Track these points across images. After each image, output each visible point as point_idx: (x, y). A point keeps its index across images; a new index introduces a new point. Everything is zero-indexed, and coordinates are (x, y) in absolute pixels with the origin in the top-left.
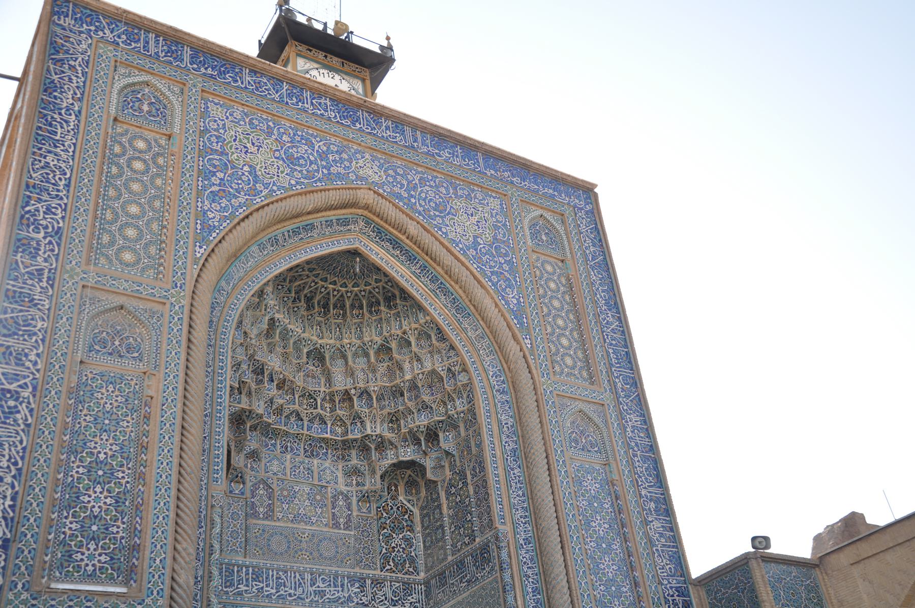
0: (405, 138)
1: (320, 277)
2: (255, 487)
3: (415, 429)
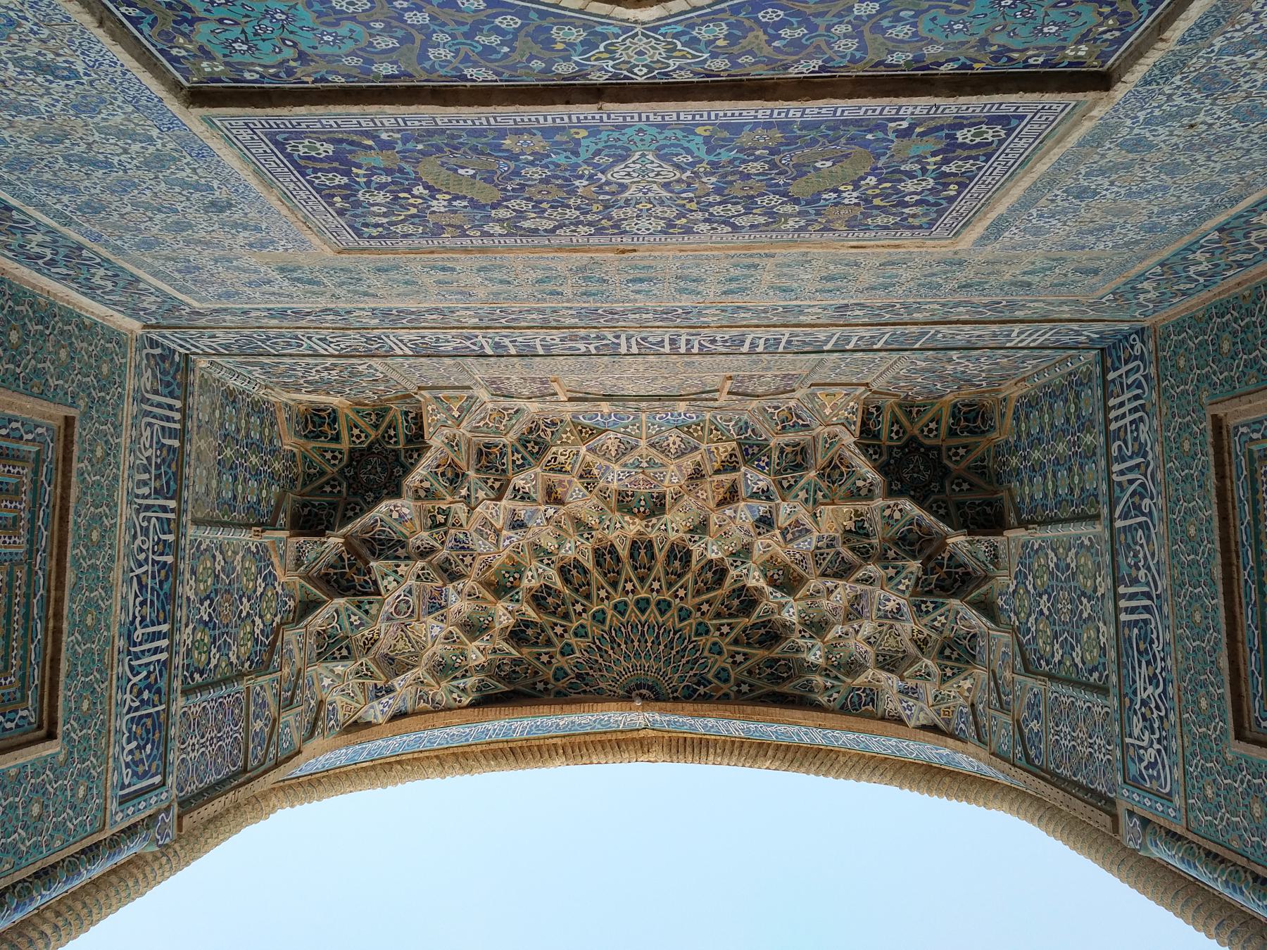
1: (673, 612)
3: (402, 569)
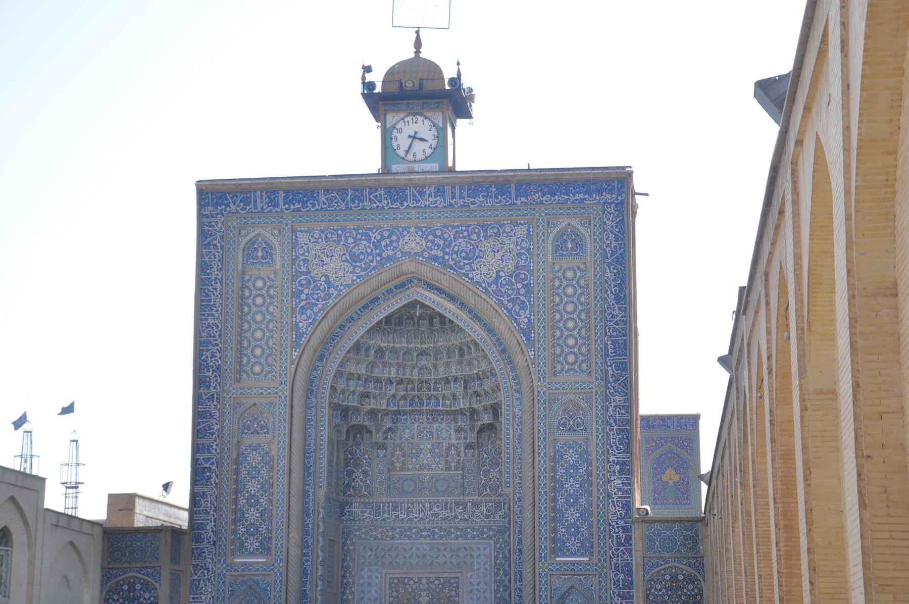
0: (444, 199)
2: (394, 449)
